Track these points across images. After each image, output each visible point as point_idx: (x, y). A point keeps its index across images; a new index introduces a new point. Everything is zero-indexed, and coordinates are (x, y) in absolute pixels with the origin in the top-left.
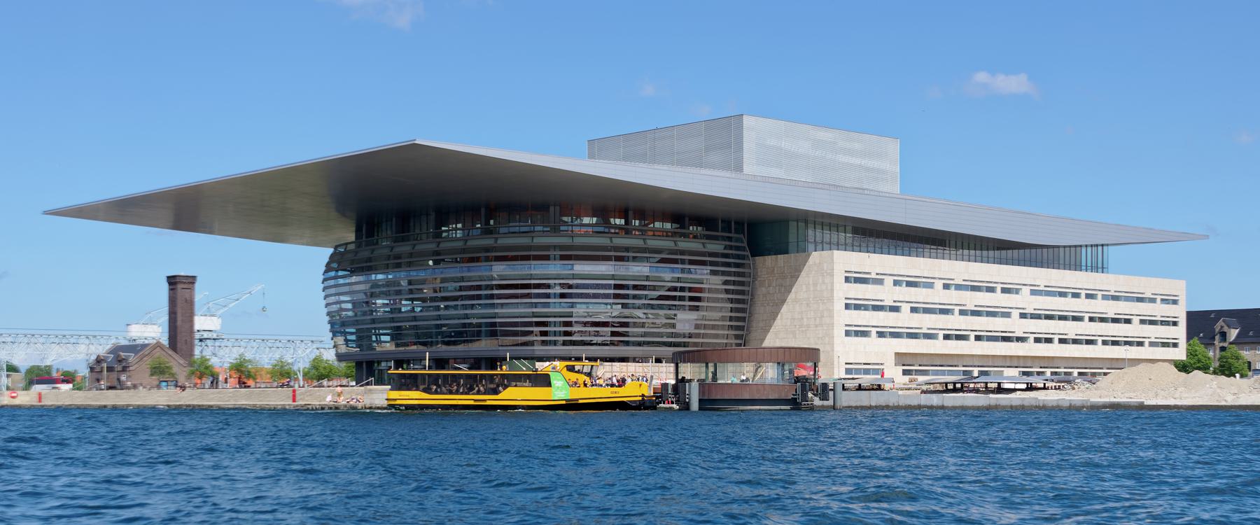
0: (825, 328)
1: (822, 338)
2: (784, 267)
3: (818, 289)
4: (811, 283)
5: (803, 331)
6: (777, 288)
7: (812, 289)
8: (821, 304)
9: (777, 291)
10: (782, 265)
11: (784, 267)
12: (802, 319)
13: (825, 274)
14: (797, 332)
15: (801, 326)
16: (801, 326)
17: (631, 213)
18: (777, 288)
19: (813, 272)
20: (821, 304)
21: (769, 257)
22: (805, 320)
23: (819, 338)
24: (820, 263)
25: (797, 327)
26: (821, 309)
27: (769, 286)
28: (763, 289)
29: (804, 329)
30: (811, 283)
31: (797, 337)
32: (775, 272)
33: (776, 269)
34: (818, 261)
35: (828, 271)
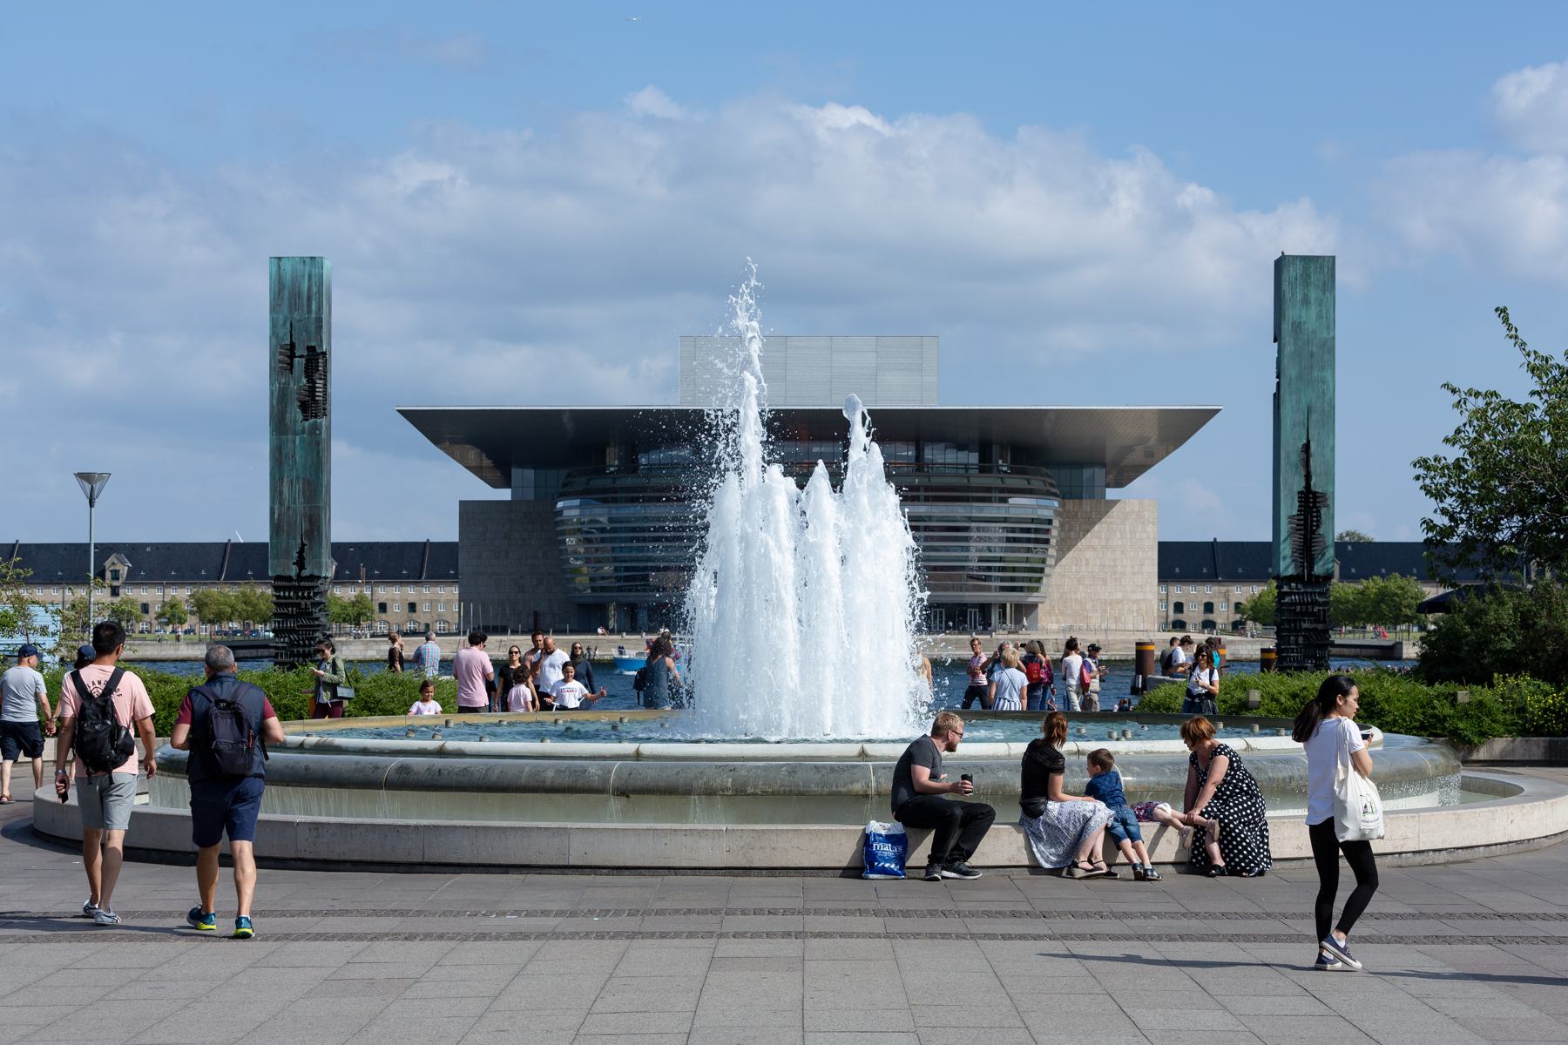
2: (1091, 512)
4: (1127, 529)
5: (1115, 578)
7: (1128, 536)
8: (1140, 553)
10: (1089, 510)
11: (1091, 512)
12: (1115, 566)
15: (1115, 573)
17: (995, 449)
18: (1081, 533)
20: (1140, 553)
21: (1071, 501)
22: (1119, 567)
27: (1071, 530)
30: (1127, 529)
32: (1079, 516)
33: (1079, 513)
34: (1136, 509)
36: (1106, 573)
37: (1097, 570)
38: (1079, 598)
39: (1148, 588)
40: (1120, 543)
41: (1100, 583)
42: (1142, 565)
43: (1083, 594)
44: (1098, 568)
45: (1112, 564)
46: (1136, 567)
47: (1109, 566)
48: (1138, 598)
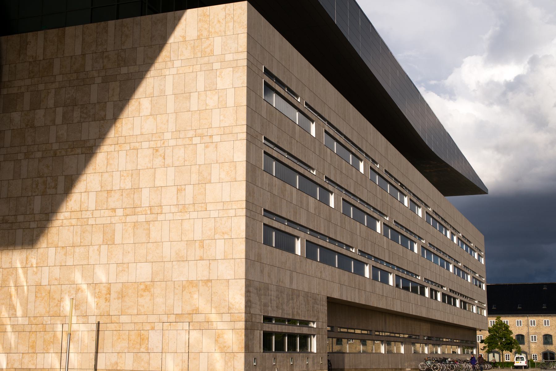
0: (214, 214)
1: (202, 241)
2: (83, 55)
3: (194, 107)
4: (169, 90)
5: (135, 225)
6: (60, 110)
8: (200, 147)
9: (59, 120)
10: (78, 52)
11: (83, 55)
12: (136, 189)
13: (216, 66)
14: (119, 227)
15: (134, 209)
16: (134, 209)
18: (60, 110)
19: (177, 64)
20: (200, 147)
22: (145, 193)
23: (190, 243)
24: (199, 38)
25: (120, 212)
26: (200, 160)
28: (16, 116)
29: (142, 218)
30: (169, 90)
31: (118, 240)
35: (229, 57)
36: (114, 210)
37: (92, 206)
38: (45, 282)
39: (220, 244)
40: (149, 126)
41: (98, 238)
42: (205, 181)
43: (57, 272)
44: (92, 196)
45: (129, 186)
46: (189, 189)
47: (122, 190)
48: (193, 277)
